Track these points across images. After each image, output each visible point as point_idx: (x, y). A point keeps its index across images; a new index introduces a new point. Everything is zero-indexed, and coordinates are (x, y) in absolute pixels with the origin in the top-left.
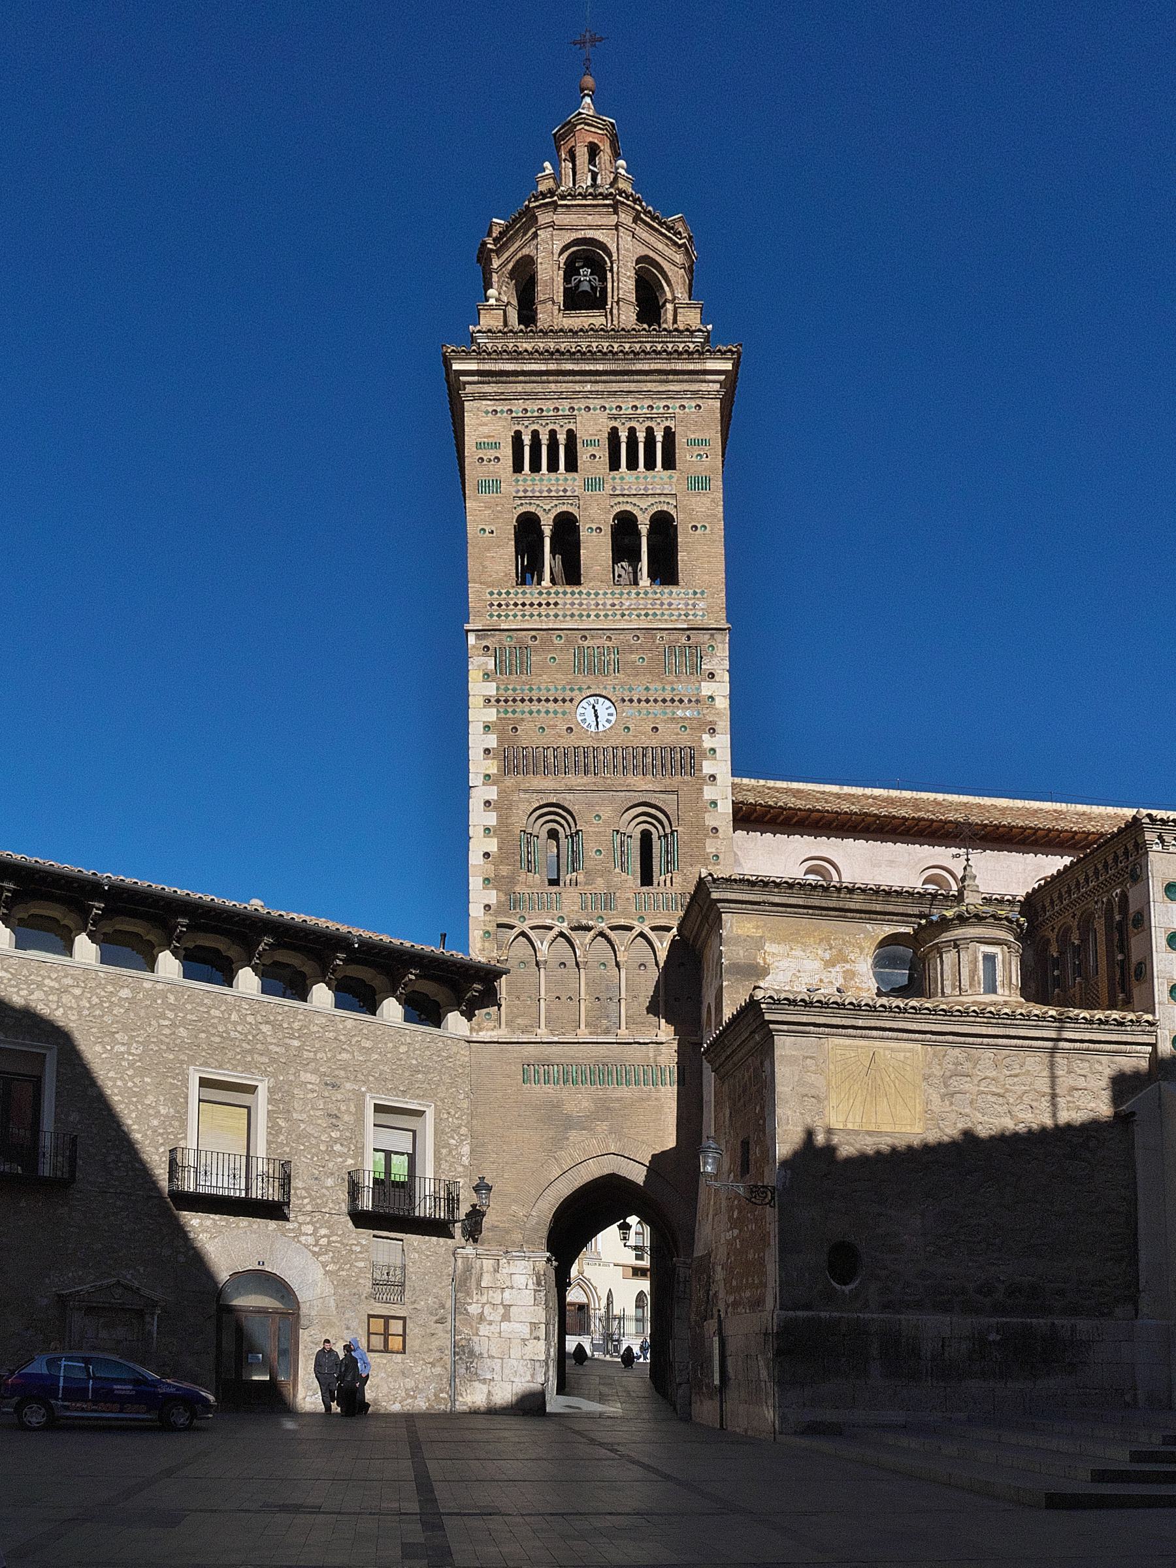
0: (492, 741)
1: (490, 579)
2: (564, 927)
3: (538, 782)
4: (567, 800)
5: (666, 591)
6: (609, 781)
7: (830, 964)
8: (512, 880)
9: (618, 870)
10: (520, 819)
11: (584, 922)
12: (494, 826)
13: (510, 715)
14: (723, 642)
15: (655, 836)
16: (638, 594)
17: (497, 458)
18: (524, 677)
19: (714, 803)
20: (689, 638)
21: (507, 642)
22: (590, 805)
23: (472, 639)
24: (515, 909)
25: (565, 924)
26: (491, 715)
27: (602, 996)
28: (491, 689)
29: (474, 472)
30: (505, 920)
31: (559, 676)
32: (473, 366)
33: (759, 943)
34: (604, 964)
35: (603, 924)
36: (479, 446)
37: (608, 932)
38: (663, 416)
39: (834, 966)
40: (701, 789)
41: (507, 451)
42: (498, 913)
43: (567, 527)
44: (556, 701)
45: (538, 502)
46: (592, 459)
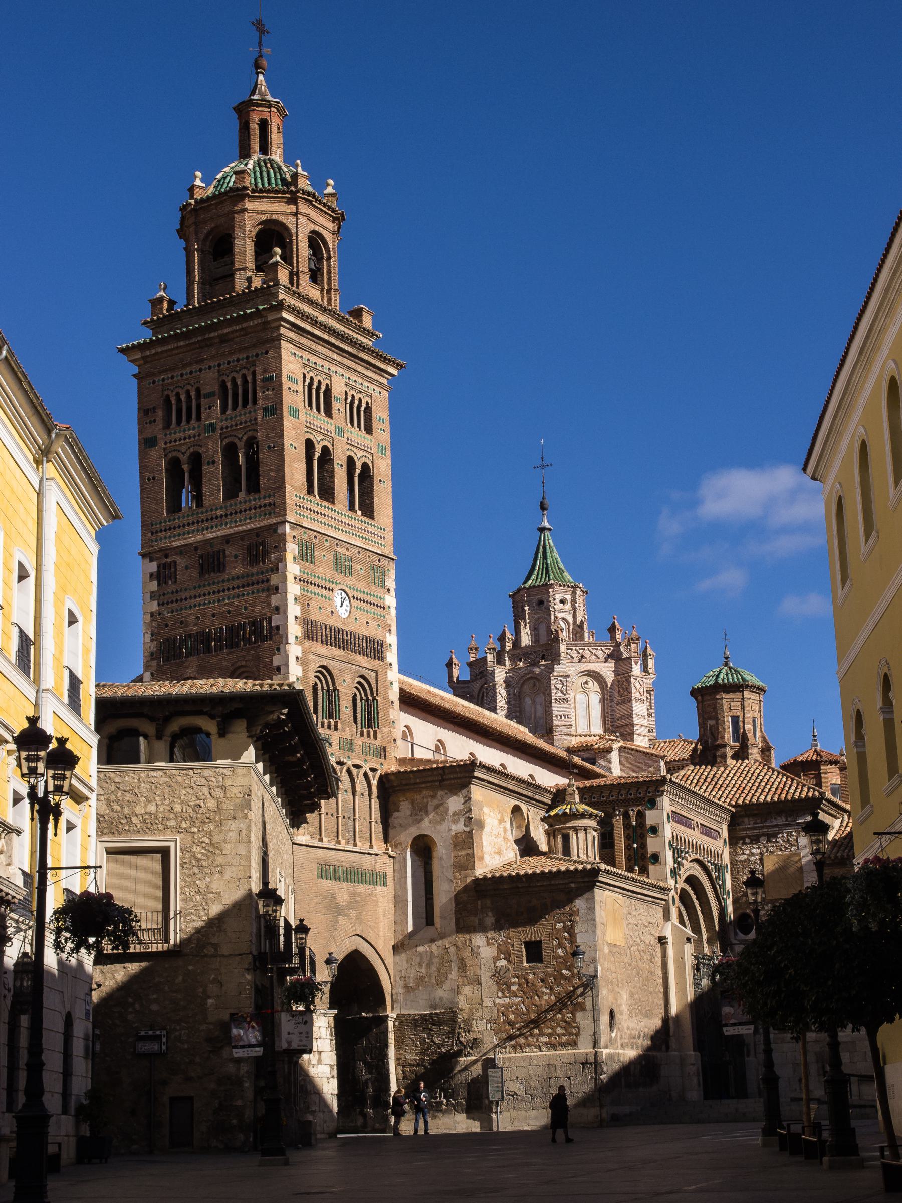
1: (295, 485)
4: (331, 664)
11: (342, 759)
13: (306, 593)
15: (358, 698)
17: (297, 392)
18: (312, 566)
20: (379, 560)
22: (342, 671)
32: (291, 318)
35: (350, 763)
36: (289, 378)
37: (352, 768)
40: (386, 672)
41: (300, 388)
45: (314, 433)
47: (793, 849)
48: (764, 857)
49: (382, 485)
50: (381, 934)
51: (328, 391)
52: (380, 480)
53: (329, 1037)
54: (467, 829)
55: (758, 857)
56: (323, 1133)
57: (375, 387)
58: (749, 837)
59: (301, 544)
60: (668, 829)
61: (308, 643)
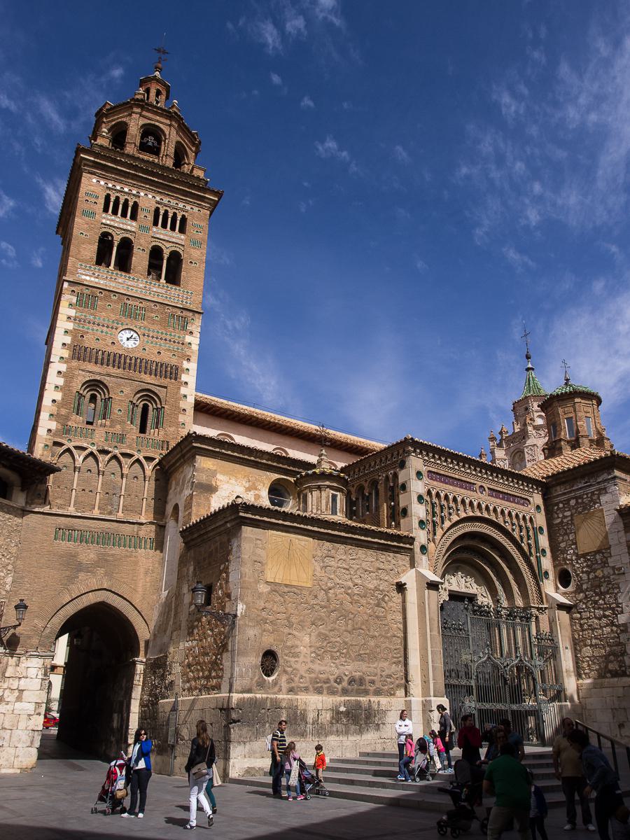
0: (68, 340)
2: (94, 449)
3: (90, 367)
4: (106, 380)
5: (174, 288)
6: (131, 374)
7: (248, 489)
8: (67, 418)
9: (129, 422)
10: (77, 385)
11: (106, 448)
12: (61, 386)
13: (81, 329)
14: (199, 319)
15: (151, 408)
16: (159, 285)
19: (185, 396)
21: (86, 292)
23: (66, 285)
24: (66, 434)
25: (95, 448)
26: (70, 326)
27: (111, 492)
28: (72, 313)
29: (81, 205)
30: (59, 440)
31: (112, 315)
33: (214, 474)
34: (113, 474)
37: (119, 456)
38: (182, 210)
39: (250, 491)
41: (102, 201)
42: (55, 435)
43: (126, 245)
44: (108, 327)
46: (146, 217)
47: (596, 506)
48: (574, 518)
49: (193, 265)
50: (140, 589)
51: (136, 205)
52: (192, 262)
53: (40, 676)
54: (191, 492)
55: (569, 518)
56: (13, 768)
57: (193, 207)
58: (561, 502)
59: (80, 296)
60: (417, 487)
61: (75, 363)
